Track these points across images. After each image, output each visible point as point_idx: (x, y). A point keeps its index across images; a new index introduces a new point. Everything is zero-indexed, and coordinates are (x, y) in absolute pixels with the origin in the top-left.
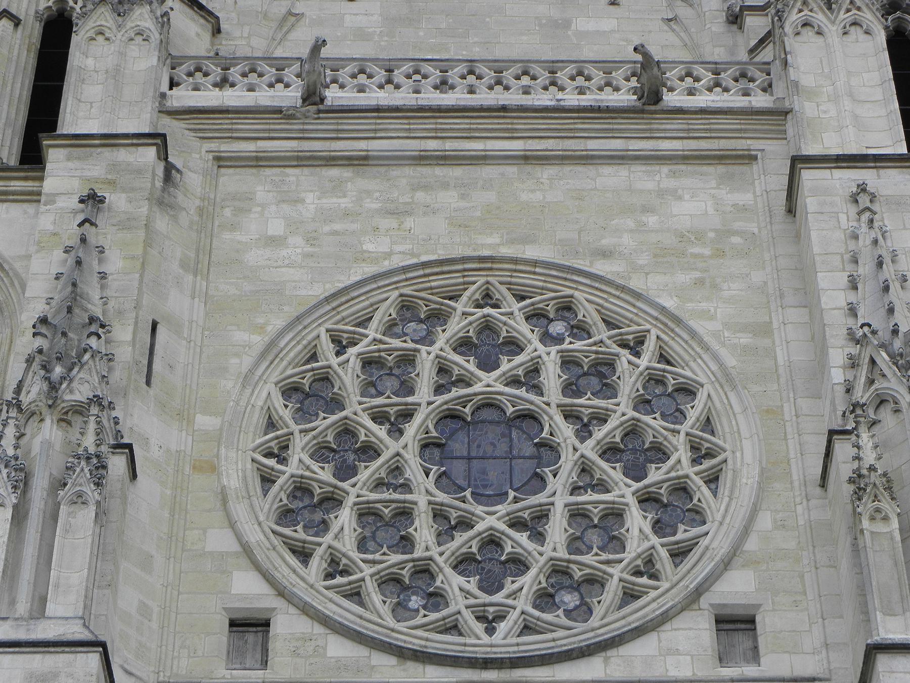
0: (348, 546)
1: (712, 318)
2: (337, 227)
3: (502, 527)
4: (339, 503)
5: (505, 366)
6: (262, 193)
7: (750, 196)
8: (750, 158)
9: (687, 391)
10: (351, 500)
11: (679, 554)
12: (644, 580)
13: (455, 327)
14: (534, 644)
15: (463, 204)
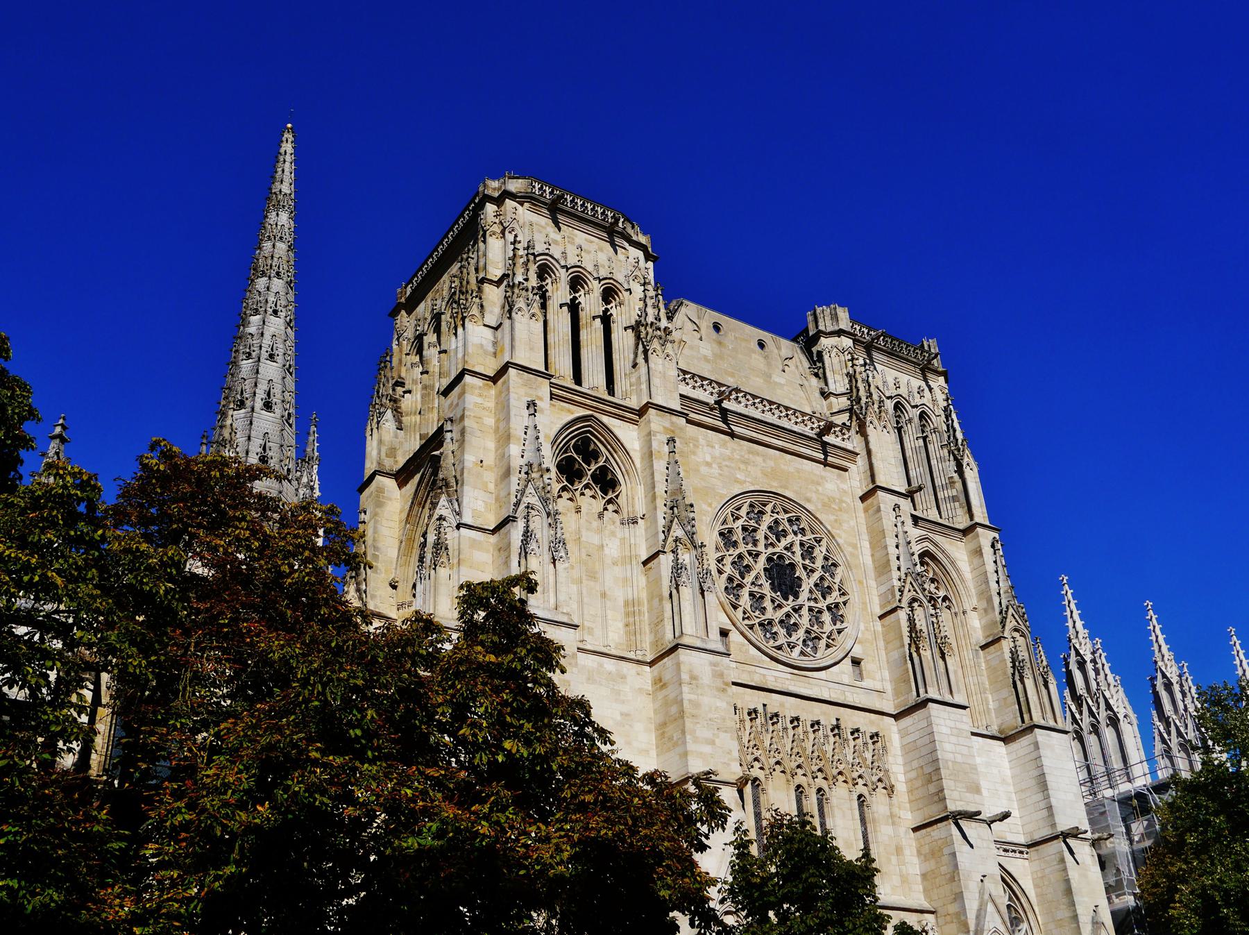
2: (727, 463)
8: (846, 470)
11: (840, 632)
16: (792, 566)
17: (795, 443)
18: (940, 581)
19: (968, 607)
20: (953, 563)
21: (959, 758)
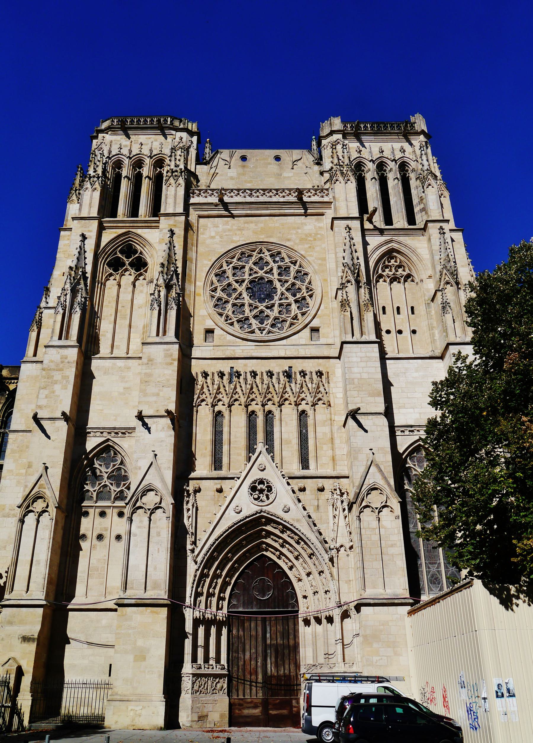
0: (230, 313)
1: (313, 256)
2: (227, 233)
3: (264, 309)
4: (229, 302)
5: (265, 269)
6: (209, 225)
7: (322, 224)
8: (323, 215)
9: (306, 274)
10: (231, 303)
11: (303, 314)
12: (295, 321)
13: (253, 259)
14: (271, 337)
15: (256, 227)
16: (270, 282)
17: (281, 208)
18: (406, 265)
19: (424, 277)
20: (414, 252)
21: (365, 376)
